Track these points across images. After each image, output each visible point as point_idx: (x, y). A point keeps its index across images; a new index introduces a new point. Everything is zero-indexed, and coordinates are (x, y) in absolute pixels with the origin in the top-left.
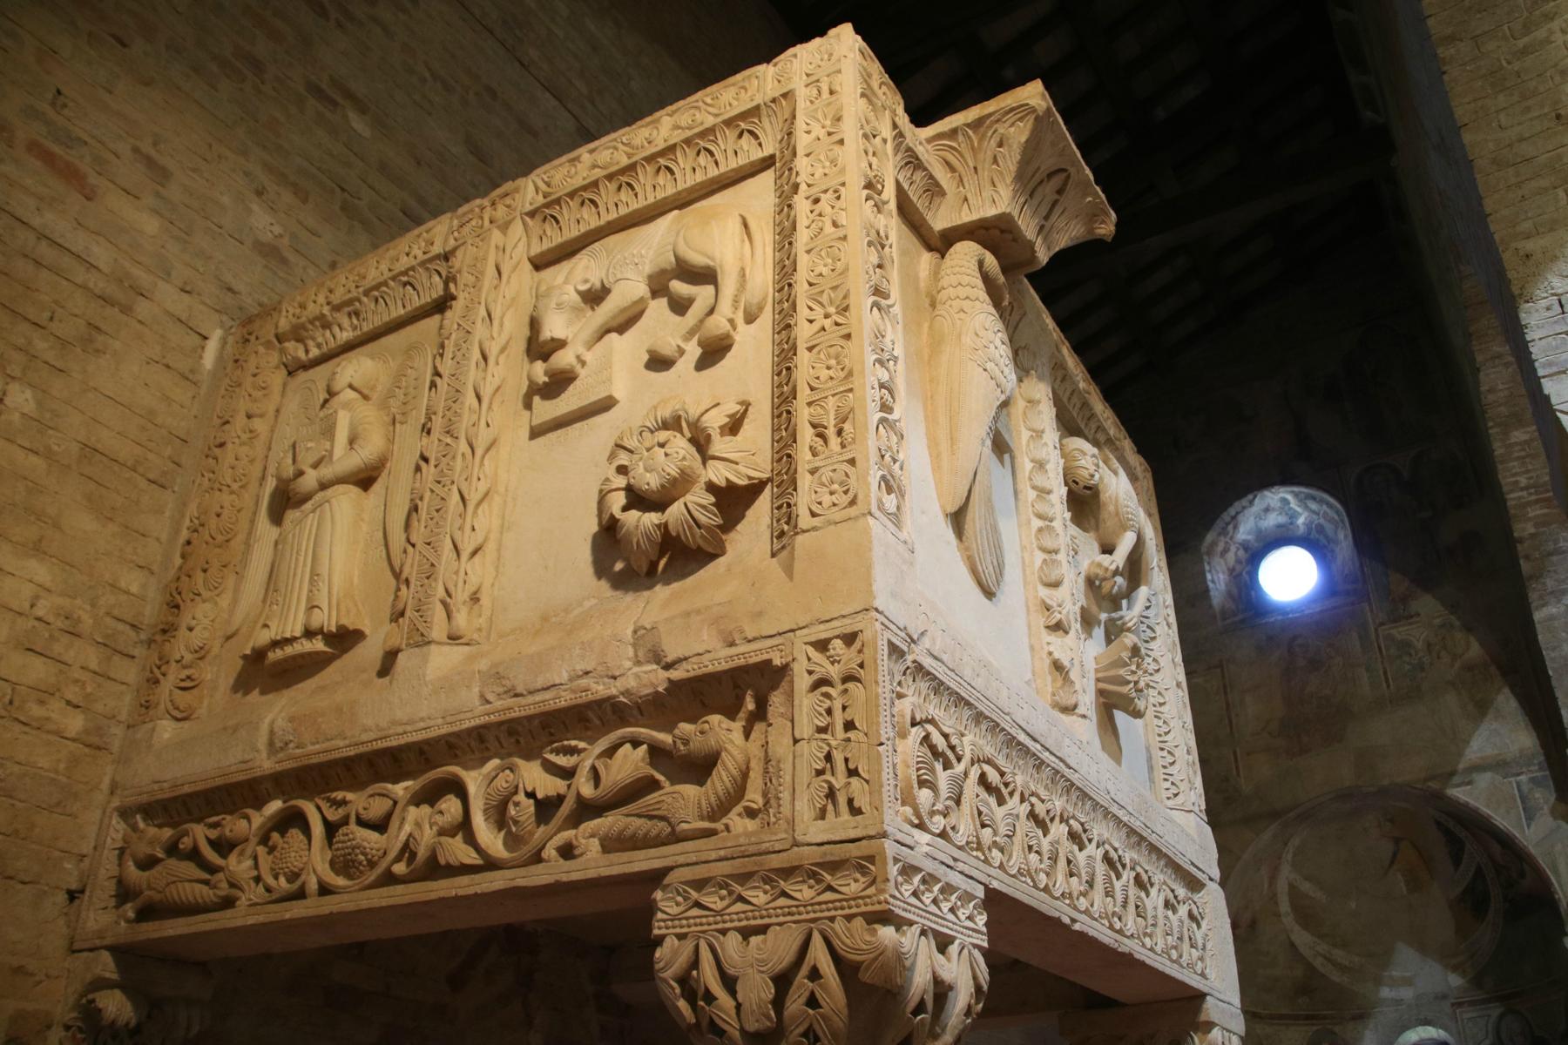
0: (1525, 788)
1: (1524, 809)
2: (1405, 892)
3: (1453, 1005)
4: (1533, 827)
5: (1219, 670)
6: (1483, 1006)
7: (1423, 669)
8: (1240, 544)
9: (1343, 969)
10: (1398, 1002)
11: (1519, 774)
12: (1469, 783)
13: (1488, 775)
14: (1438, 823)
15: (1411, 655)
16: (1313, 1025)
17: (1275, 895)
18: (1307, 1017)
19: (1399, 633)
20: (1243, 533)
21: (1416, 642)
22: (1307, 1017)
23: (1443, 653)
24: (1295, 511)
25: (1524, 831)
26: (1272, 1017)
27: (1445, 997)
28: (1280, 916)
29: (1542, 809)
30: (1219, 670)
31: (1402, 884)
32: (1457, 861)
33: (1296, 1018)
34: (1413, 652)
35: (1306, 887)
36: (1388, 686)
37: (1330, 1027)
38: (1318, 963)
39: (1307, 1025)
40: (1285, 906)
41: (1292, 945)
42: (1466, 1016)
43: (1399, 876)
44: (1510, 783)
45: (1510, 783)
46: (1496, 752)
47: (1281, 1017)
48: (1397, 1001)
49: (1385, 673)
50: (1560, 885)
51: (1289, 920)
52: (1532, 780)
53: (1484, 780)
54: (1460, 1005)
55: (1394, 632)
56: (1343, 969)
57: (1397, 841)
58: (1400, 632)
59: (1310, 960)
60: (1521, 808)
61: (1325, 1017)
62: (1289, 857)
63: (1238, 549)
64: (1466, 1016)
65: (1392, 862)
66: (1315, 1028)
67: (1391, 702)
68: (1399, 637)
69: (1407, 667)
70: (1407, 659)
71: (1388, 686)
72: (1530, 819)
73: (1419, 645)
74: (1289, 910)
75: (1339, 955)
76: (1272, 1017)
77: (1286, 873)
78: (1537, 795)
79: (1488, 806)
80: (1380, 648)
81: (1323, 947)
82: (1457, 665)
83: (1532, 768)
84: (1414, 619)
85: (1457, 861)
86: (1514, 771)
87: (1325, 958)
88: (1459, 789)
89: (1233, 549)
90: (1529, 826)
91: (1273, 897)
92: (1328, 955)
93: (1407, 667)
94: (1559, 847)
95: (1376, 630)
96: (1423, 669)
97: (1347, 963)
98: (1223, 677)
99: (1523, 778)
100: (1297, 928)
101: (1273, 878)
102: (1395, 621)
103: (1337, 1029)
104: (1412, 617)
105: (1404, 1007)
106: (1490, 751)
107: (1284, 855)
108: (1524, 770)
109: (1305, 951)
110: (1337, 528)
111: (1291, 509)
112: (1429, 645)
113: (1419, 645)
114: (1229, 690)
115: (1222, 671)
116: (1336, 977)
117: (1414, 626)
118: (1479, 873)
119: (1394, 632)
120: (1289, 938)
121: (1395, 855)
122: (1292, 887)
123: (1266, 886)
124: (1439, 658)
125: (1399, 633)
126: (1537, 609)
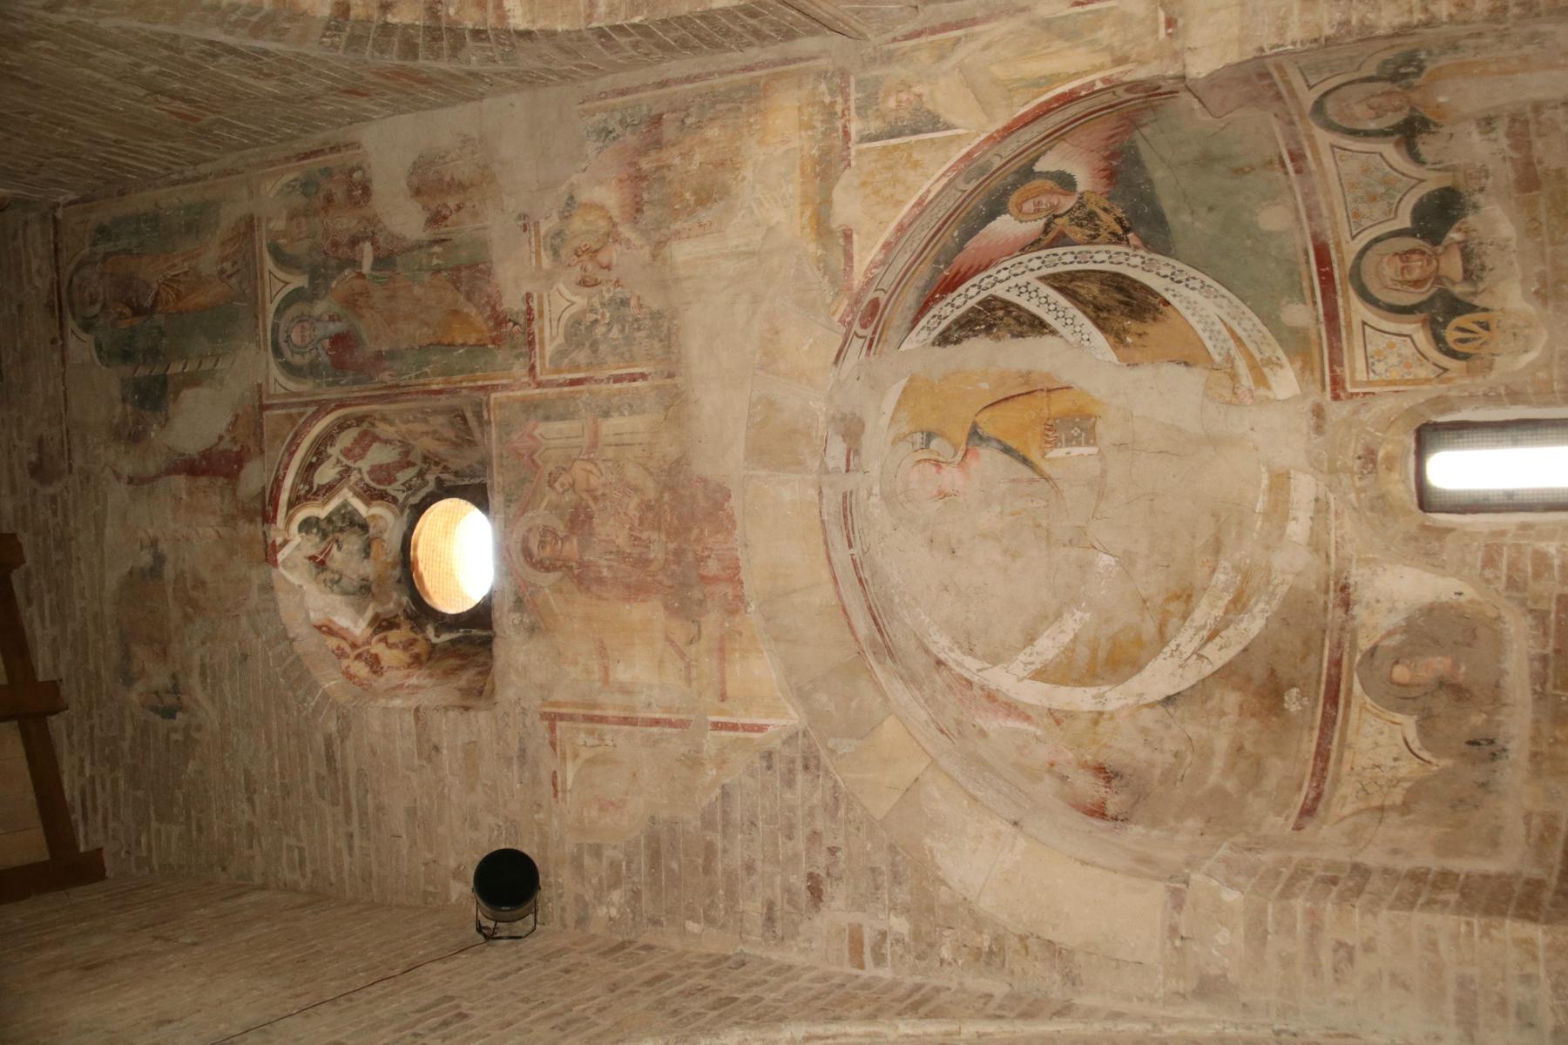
0: (875, 126)
1: (916, 132)
2: (1093, 450)
3: (1336, 397)
4: (953, 119)
5: (560, 724)
6: (1344, 334)
7: (624, 303)
8: (375, 633)
9: (1239, 604)
10: (1320, 507)
11: (846, 133)
12: (848, 236)
13: (837, 194)
14: (944, 339)
15: (596, 321)
16: (1350, 691)
17: (1051, 712)
18: (1332, 697)
19: (553, 339)
20: (355, 623)
21: (574, 309)
22: (1332, 697)
23: (603, 258)
24: (337, 510)
25: (959, 136)
26: (1320, 774)
27: (1318, 412)
28: (1101, 713)
29: (920, 96)
30: (560, 724)
31: (1076, 451)
32: (1037, 326)
33: (1328, 722)
34: (592, 317)
35: (1048, 647)
36: (643, 376)
37: (1358, 658)
38: (1218, 656)
39: (1348, 704)
40: (1082, 699)
41: (1169, 700)
42: (1361, 375)
43: (1058, 453)
44: (859, 153)
45: (859, 153)
46: (797, 174)
47: (1322, 755)
48: (1317, 511)
49: (618, 379)
50: (1077, 75)
51: (1116, 697)
52: (861, 111)
53: (847, 206)
54: (1337, 382)
55: (549, 349)
56: (1239, 604)
57: (975, 435)
58: (551, 337)
59: (1208, 670)
60: (913, 138)
61: (1337, 663)
62: (972, 663)
63: (384, 640)
64: (1361, 375)
65: (1025, 461)
66: (1357, 687)
67: (671, 376)
68: (560, 340)
69: (615, 333)
70: (600, 330)
71: (643, 376)
72: (935, 122)
73: (580, 302)
74: (1093, 691)
75: (1206, 612)
76: (1320, 774)
77: (1010, 680)
78: (892, 103)
79: (898, 204)
80: (573, 383)
81: (1186, 640)
82: (626, 231)
83: (839, 109)
84: (534, 305)
85: (1037, 326)
86: (839, 143)
87: (1211, 638)
88: (856, 258)
89: (378, 648)
90: (948, 127)
91: (1058, 718)
92: (1205, 633)
93: (615, 333)
94: (998, 71)
95: (540, 385)
96: (624, 303)
97: (1228, 597)
98: (571, 718)
99: (854, 128)
100: (1135, 684)
101: (1012, 709)
102: (531, 343)
103: (1364, 644)
104: (529, 311)
105: (1332, 497)
106: (793, 188)
107: (967, 675)
108: (839, 124)
109: (1190, 678)
110: (376, 438)
111: (329, 519)
112: (583, 283)
113: (580, 302)
114: (597, 712)
115: (562, 717)
116: (1252, 625)
117: (546, 306)
118: (1064, 284)
119: (549, 349)
120: (1151, 706)
121: (1007, 450)
122: (1040, 675)
123: (1025, 726)
124: (608, 267)
125: (553, 339)
126: (502, 16)
